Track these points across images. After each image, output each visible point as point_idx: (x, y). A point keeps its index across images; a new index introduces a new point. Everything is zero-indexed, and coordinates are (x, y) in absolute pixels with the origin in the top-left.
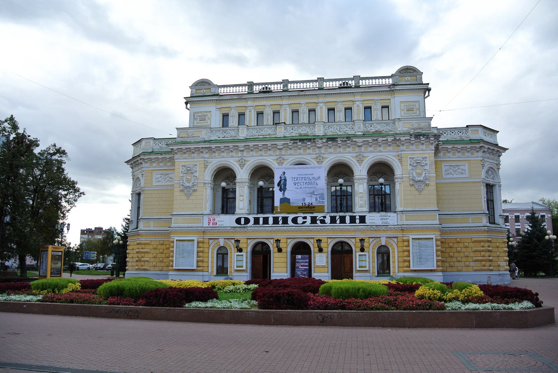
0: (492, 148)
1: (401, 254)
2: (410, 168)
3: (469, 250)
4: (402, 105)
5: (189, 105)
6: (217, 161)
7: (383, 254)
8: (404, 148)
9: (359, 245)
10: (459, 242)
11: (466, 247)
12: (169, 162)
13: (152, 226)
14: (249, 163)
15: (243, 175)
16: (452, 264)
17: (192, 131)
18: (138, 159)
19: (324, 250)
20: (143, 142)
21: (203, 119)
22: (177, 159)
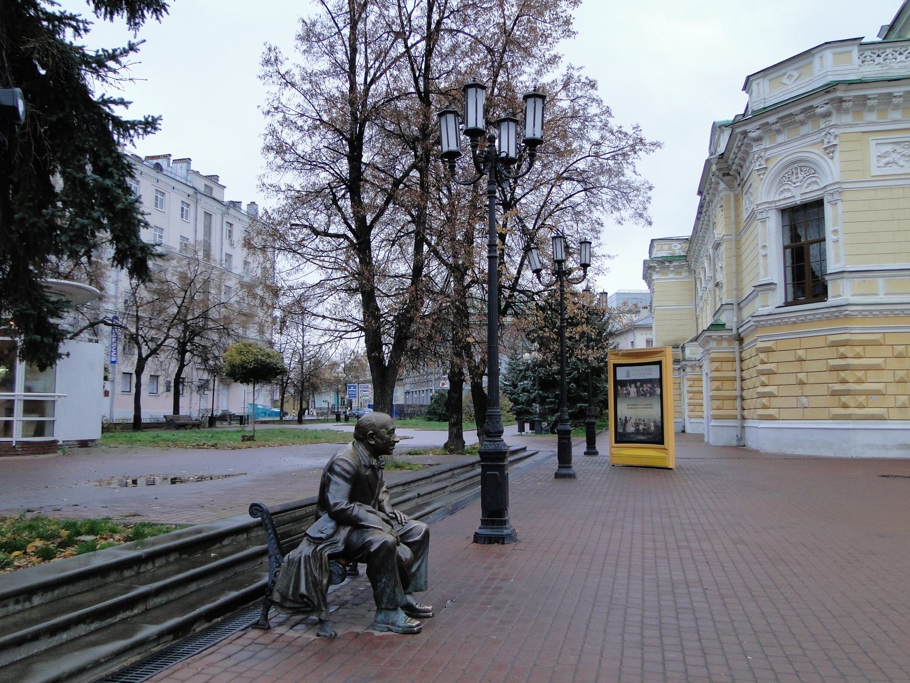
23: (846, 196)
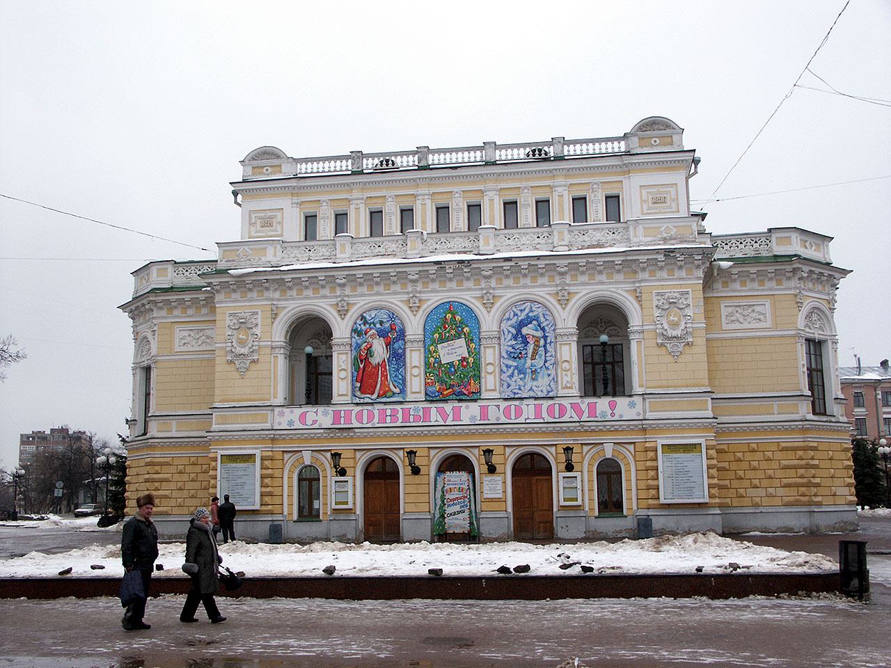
0: (817, 270)
1: (642, 475)
2: (657, 313)
3: (775, 465)
4: (644, 192)
5: (240, 197)
6: (294, 305)
7: (609, 474)
8: (646, 275)
9: (562, 458)
10: (754, 451)
11: (769, 460)
12: (204, 306)
13: (175, 430)
14: (356, 307)
15: (341, 330)
16: (742, 491)
17: (246, 248)
18: (145, 301)
19: (499, 468)
20: (154, 269)
21: (267, 223)
22: (221, 302)
23: (159, 365)
